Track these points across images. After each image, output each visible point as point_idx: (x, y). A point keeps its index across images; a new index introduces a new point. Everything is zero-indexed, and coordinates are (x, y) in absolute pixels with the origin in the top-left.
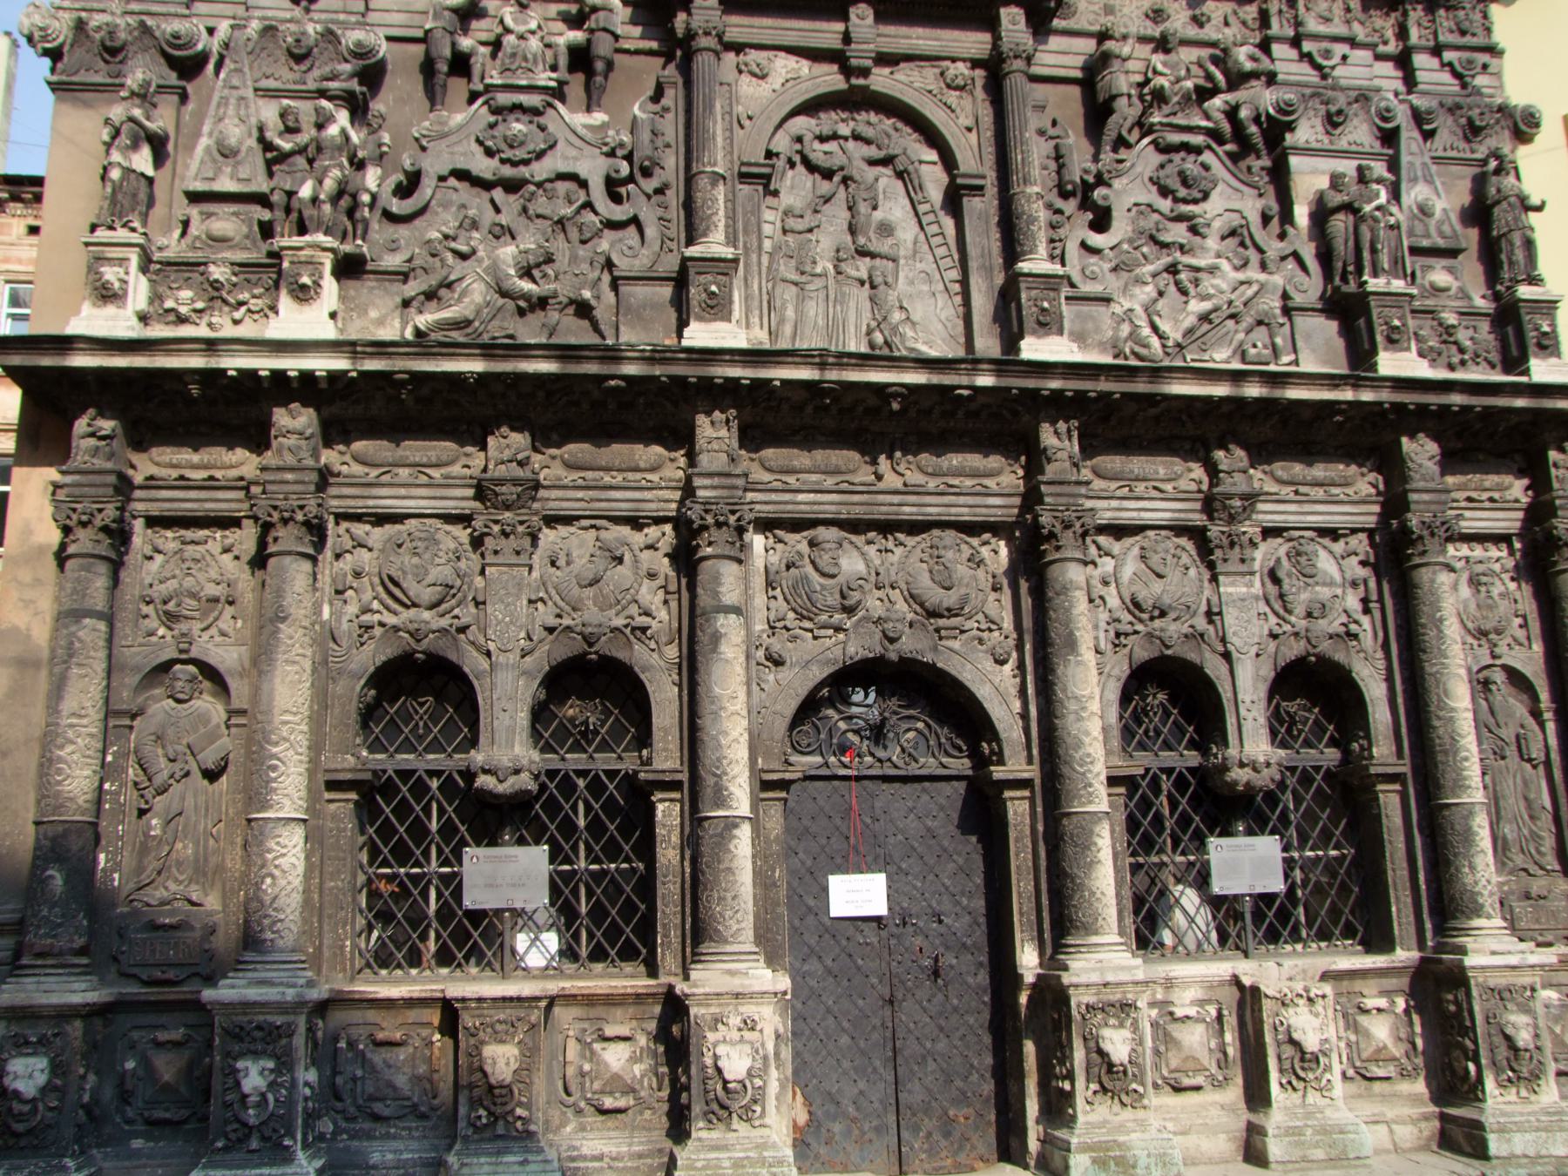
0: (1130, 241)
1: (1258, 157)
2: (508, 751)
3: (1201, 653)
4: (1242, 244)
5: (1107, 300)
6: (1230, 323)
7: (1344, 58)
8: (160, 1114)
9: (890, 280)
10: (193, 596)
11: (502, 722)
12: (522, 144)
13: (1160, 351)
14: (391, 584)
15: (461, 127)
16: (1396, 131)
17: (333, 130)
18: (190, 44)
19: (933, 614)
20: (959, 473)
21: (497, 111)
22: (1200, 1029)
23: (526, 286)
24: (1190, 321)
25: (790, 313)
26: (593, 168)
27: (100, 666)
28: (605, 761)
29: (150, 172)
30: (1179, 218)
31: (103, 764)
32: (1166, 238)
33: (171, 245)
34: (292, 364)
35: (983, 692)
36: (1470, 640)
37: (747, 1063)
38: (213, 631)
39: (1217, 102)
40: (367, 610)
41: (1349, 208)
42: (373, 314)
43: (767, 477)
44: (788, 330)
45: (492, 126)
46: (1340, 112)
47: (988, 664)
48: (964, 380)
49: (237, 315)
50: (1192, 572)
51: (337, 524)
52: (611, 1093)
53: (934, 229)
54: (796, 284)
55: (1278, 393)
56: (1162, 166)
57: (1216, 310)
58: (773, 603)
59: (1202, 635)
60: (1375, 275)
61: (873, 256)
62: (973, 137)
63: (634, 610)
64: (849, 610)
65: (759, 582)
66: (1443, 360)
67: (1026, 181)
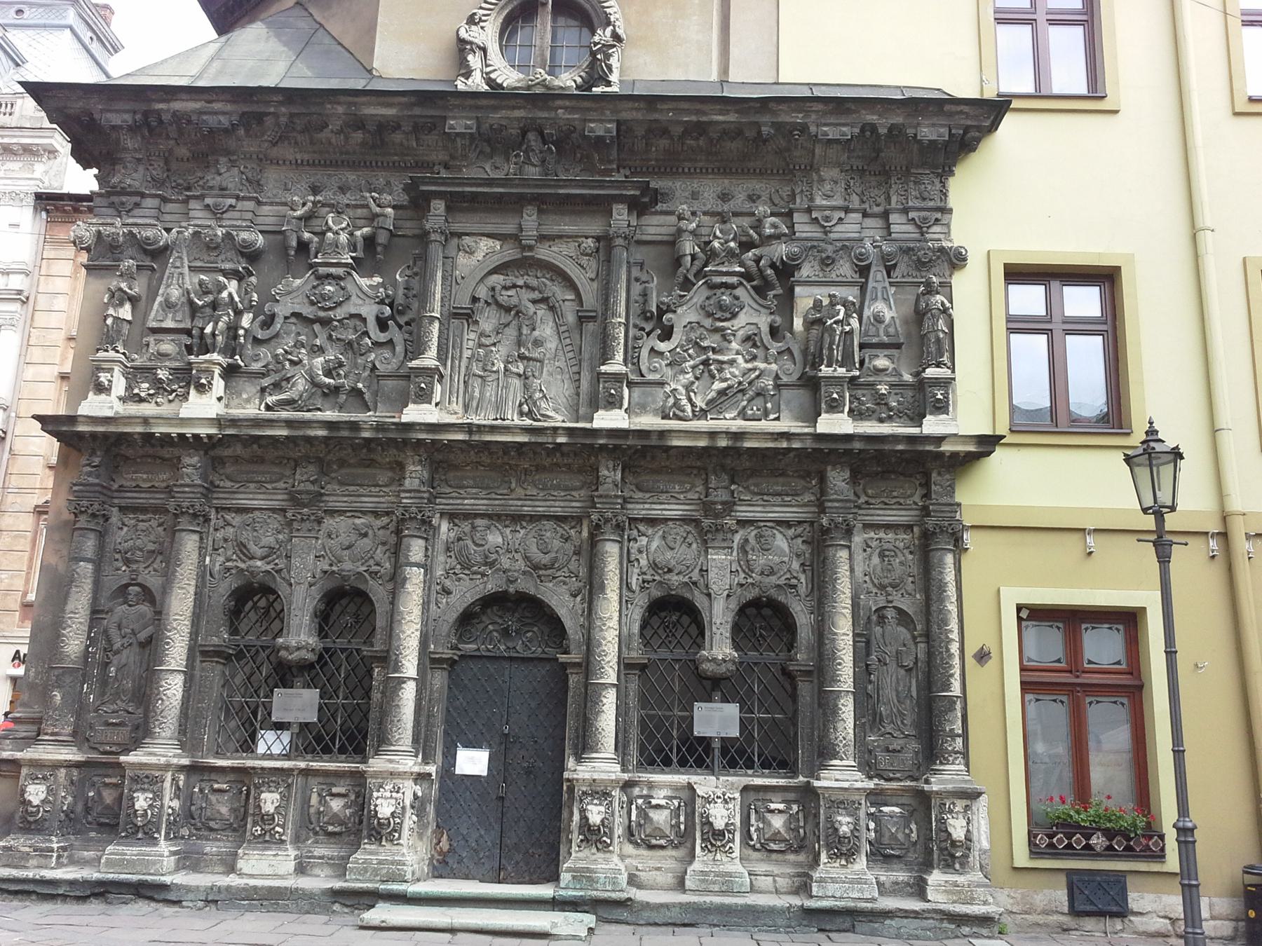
0: (682, 346)
2: (300, 637)
3: (693, 594)
4: (754, 345)
5: (661, 384)
6: (739, 395)
7: (840, 219)
8: (102, 820)
9: (536, 374)
10: (141, 550)
11: (294, 622)
12: (330, 298)
14: (242, 546)
15: (298, 288)
16: (868, 267)
17: (225, 294)
18: (156, 241)
19: (536, 567)
20: (558, 488)
21: (319, 277)
22: (667, 812)
23: (327, 380)
24: (713, 394)
25: (477, 394)
26: (369, 311)
27: (87, 586)
28: (357, 644)
29: (129, 318)
30: (717, 330)
31: (89, 638)
32: (705, 344)
33: (139, 360)
34: (189, 431)
35: (562, 613)
36: (875, 590)
37: (393, 809)
38: (151, 569)
39: (750, 254)
40: (228, 560)
41: (820, 322)
42: (245, 396)
43: (448, 490)
44: (475, 404)
45: (314, 287)
46: (828, 257)
47: (567, 597)
48: (550, 440)
49: (171, 397)
50: (694, 546)
51: (217, 512)
52: (332, 824)
53: (568, 341)
55: (738, 444)
56: (708, 298)
57: (730, 387)
58: (449, 560)
59: (695, 583)
60: (828, 366)
61: (529, 359)
62: (595, 285)
63: (371, 562)
64: (492, 565)
65: (440, 546)
66: (875, 415)
67: (614, 315)
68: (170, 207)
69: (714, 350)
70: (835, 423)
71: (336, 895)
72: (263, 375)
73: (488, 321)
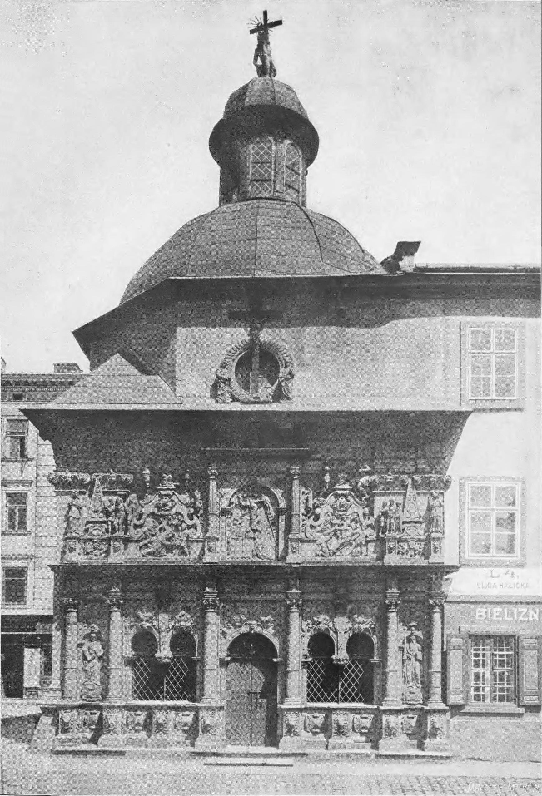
1: (365, 496)
4: (357, 523)
13: (328, 554)
23: (168, 543)
26: (185, 511)
32: (333, 522)
40: (132, 622)
54: (235, 539)
68: (90, 462)
69: (339, 525)
70: (391, 559)
71: (192, 754)
72: (141, 541)
73: (237, 513)
